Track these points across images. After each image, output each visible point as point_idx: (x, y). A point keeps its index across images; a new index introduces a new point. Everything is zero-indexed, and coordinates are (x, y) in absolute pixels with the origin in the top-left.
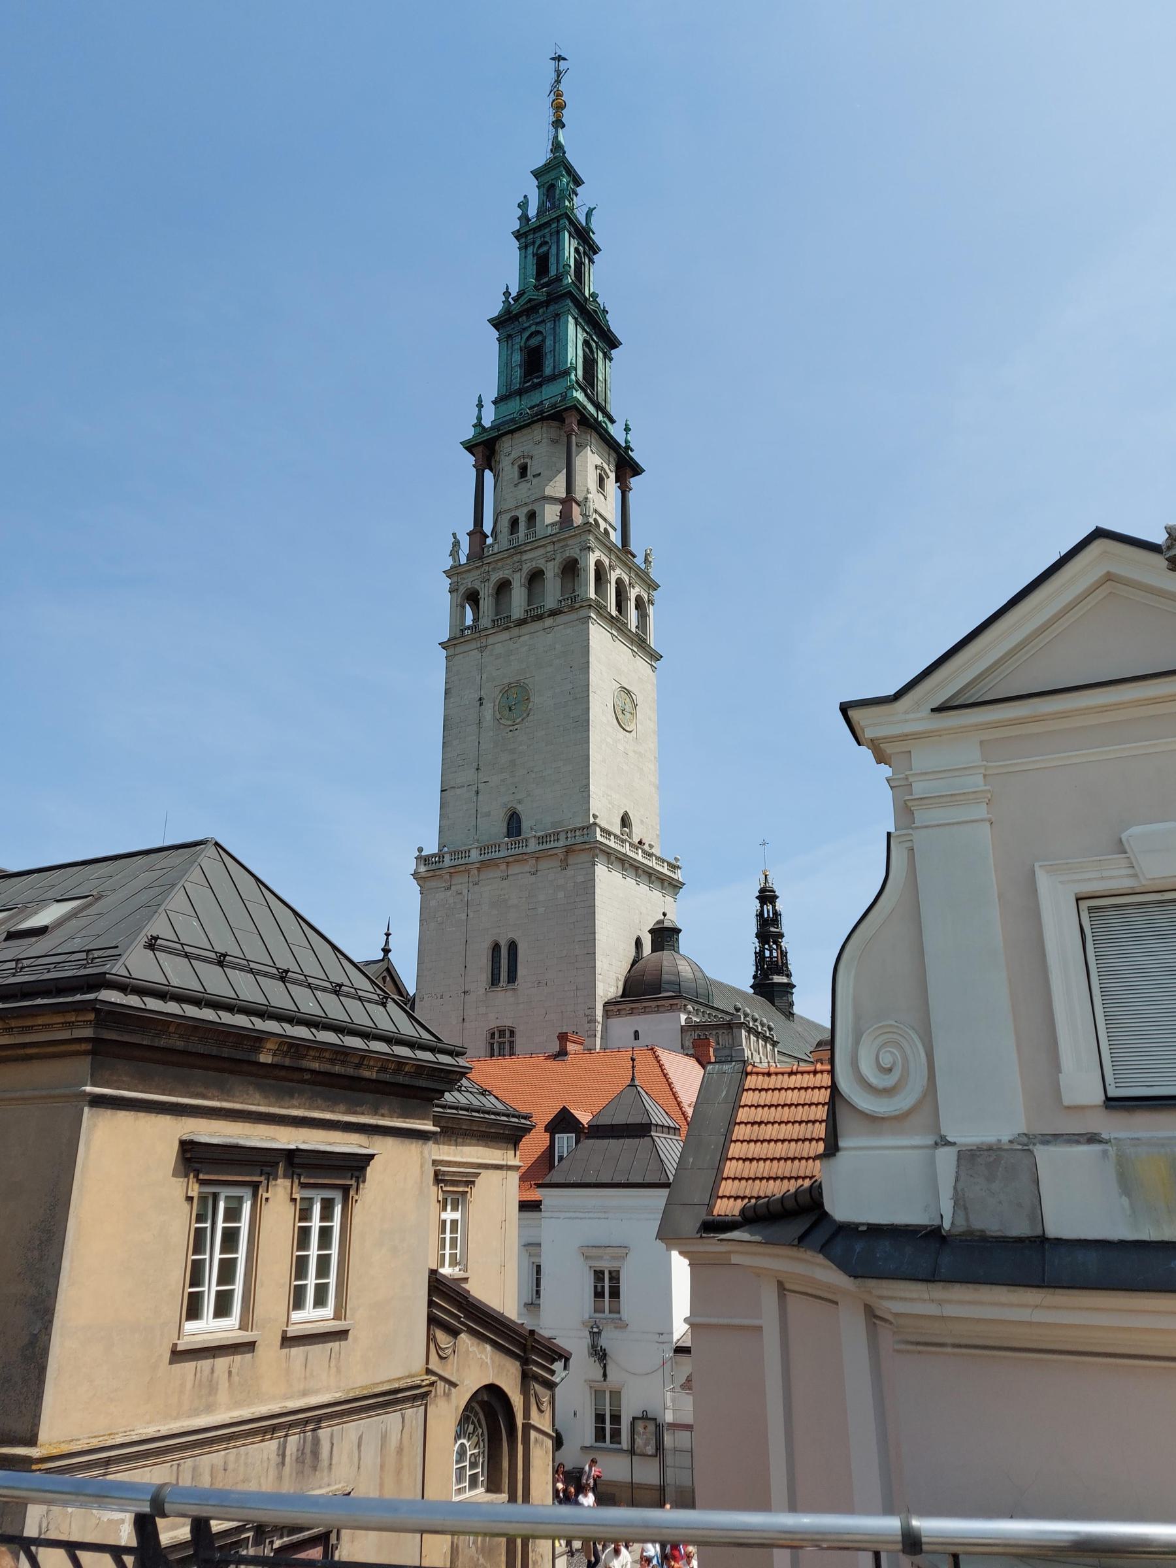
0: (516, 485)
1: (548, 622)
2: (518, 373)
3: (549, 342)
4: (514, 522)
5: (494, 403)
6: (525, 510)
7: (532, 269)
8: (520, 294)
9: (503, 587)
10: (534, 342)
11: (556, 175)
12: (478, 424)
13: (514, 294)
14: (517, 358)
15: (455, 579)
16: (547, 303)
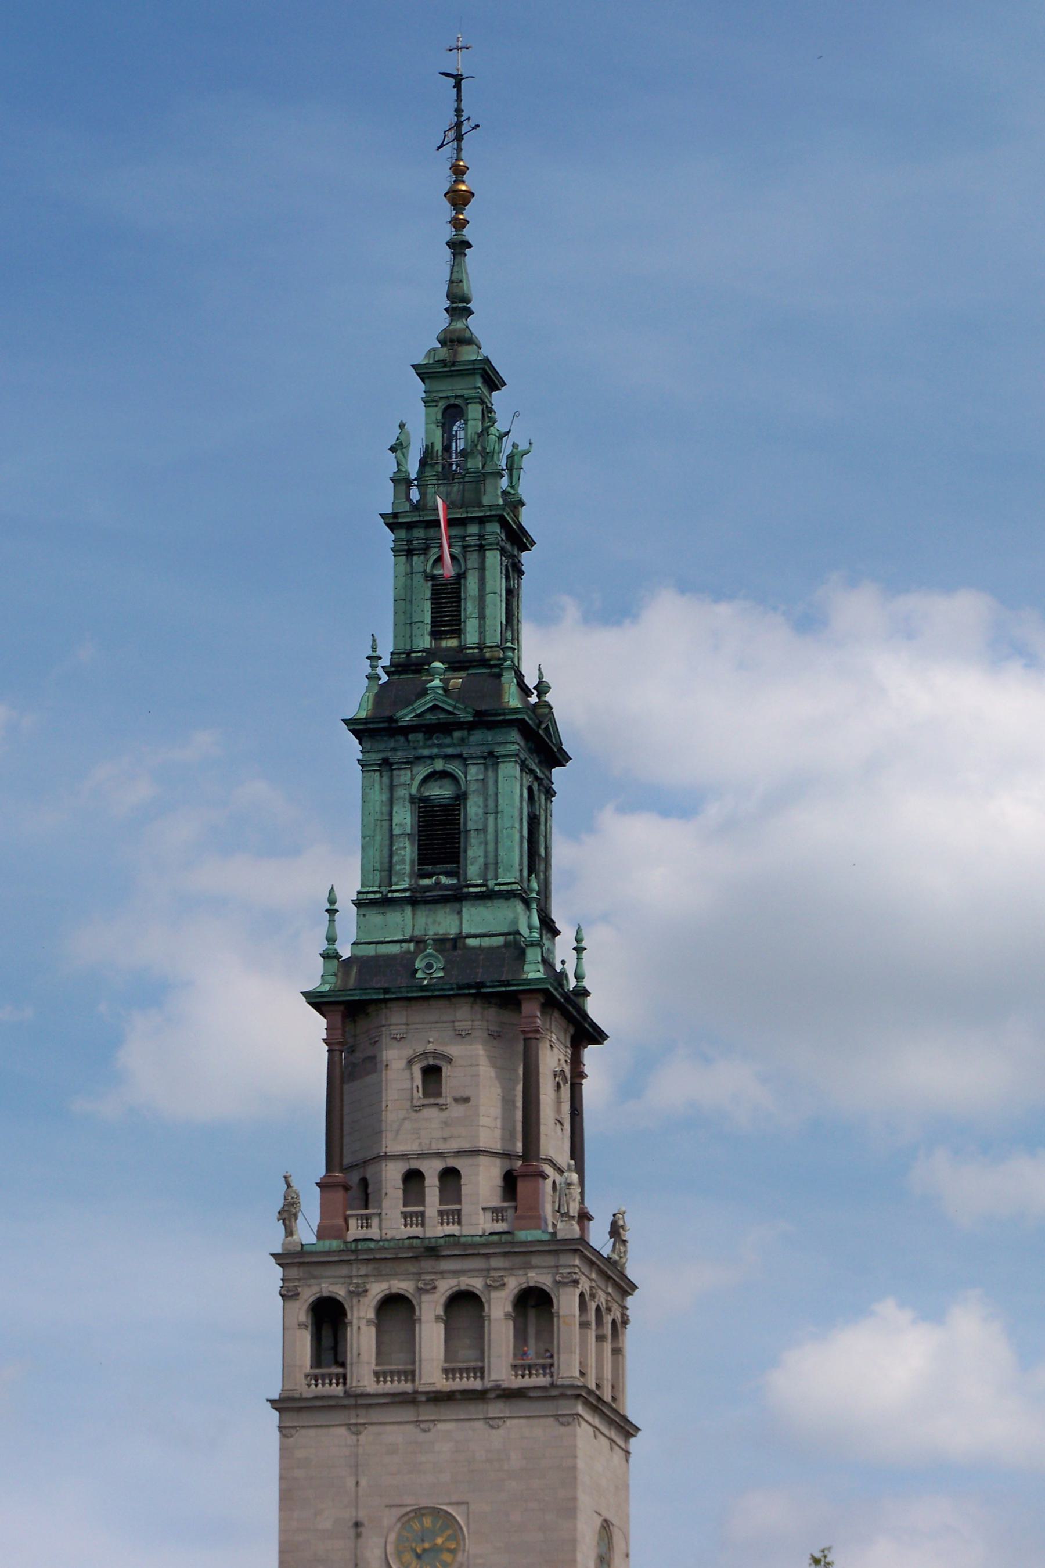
0: (417, 1109)
1: (496, 1409)
2: (407, 852)
3: (473, 809)
4: (413, 1178)
5: (359, 904)
6: (438, 1165)
8: (407, 666)
9: (396, 1308)
10: (440, 792)
11: (459, 377)
12: (329, 956)
13: (386, 661)
14: (405, 818)
15: (294, 1272)
16: (471, 727)
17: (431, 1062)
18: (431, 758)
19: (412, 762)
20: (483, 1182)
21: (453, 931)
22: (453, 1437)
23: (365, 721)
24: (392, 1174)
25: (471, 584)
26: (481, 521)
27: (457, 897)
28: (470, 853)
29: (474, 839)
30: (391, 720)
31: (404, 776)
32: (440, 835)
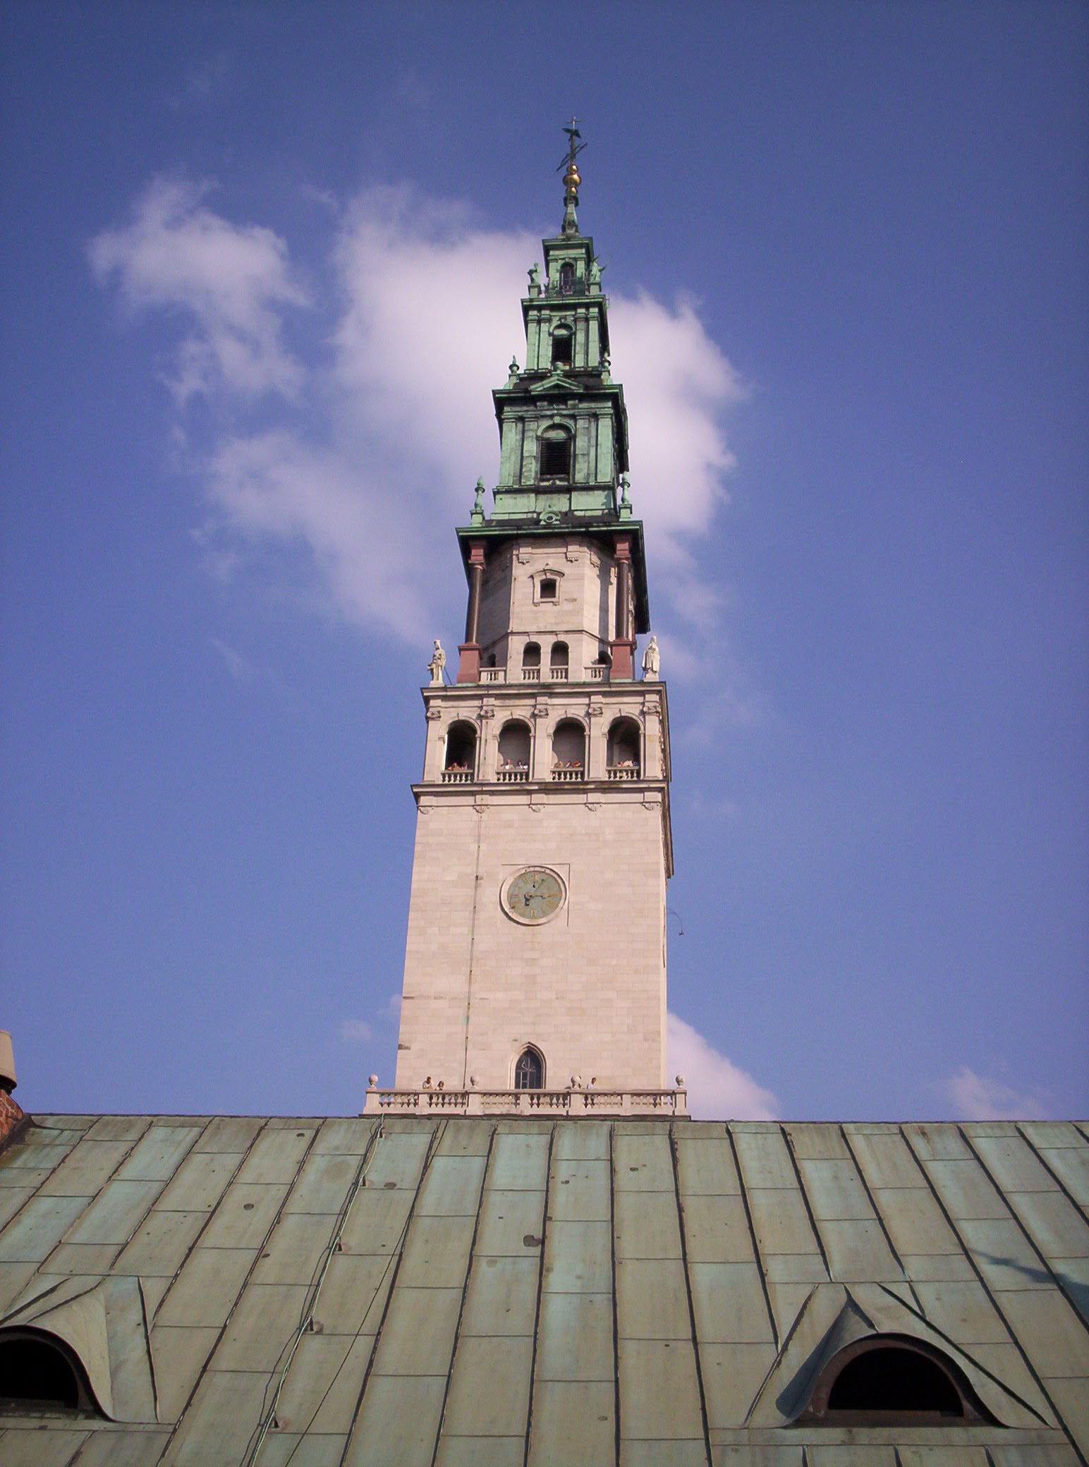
2: (532, 467)
3: (581, 443)
4: (532, 652)
6: (552, 640)
7: (547, 351)
10: (559, 435)
16: (582, 398)
17: (549, 576)
18: (552, 417)
19: (537, 418)
20: (584, 654)
21: (565, 509)
22: (562, 814)
23: (509, 392)
24: (516, 647)
25: (580, 337)
26: (587, 306)
27: (568, 490)
28: (577, 466)
29: (580, 459)
30: (527, 391)
31: (533, 425)
32: (556, 459)
